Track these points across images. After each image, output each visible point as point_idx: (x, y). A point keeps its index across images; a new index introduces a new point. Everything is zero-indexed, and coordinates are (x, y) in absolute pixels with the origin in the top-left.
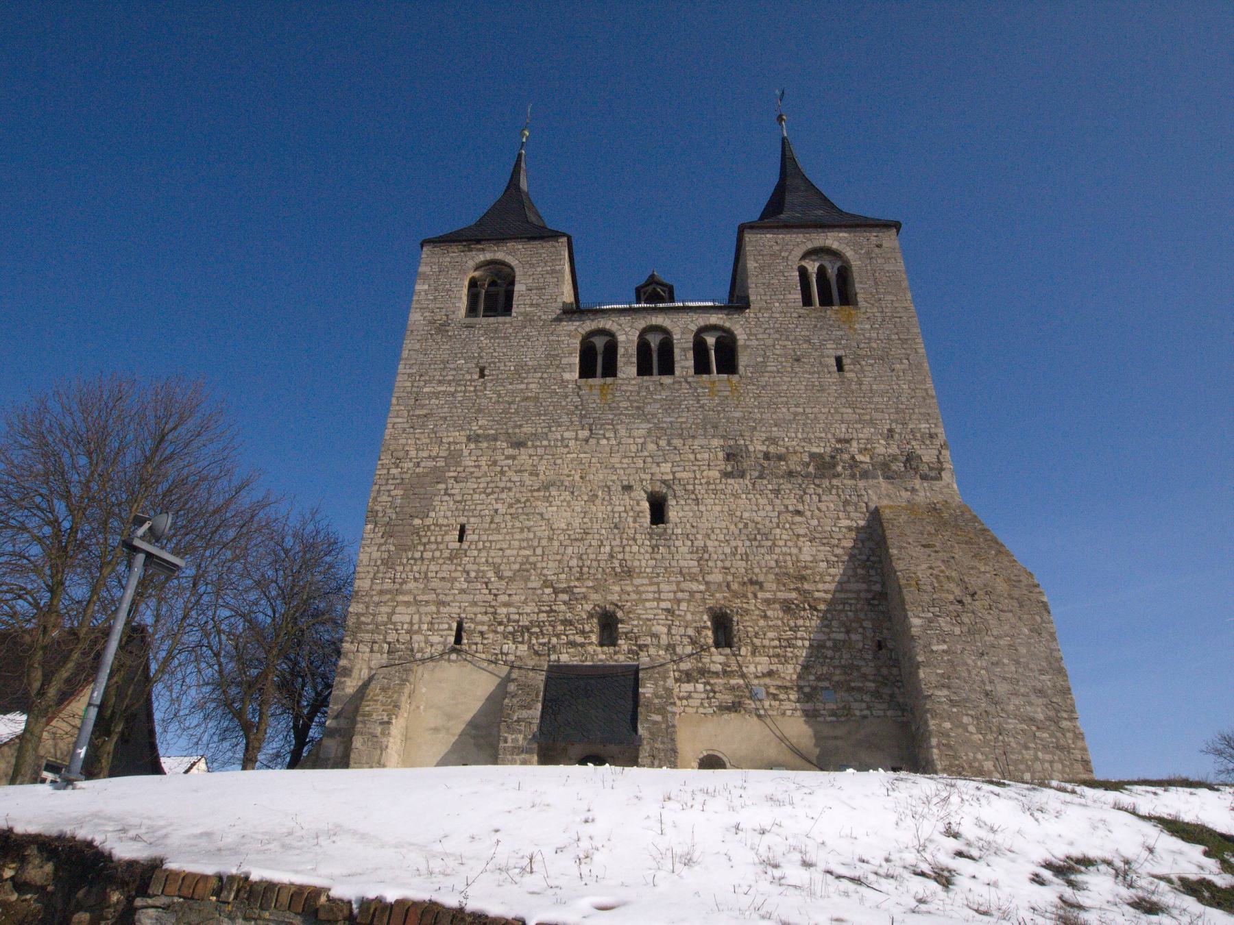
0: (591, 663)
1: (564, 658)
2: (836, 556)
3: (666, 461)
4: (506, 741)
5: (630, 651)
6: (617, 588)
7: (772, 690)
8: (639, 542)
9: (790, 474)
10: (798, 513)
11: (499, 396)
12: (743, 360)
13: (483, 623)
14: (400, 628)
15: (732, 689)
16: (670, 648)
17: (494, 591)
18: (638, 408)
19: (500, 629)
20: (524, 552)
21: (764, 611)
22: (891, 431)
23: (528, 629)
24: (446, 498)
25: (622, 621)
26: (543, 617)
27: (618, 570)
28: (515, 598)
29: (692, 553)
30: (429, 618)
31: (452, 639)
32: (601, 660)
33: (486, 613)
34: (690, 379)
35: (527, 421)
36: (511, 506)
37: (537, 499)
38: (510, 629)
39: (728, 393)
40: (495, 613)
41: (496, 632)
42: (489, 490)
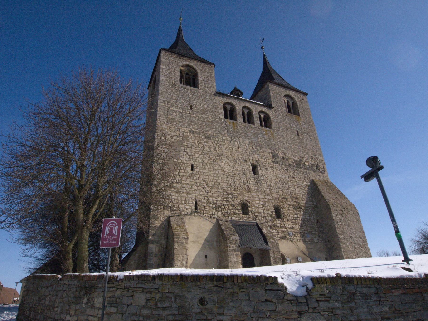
0: (242, 221)
1: (233, 218)
2: (304, 193)
3: (256, 154)
4: (230, 247)
5: (253, 217)
6: (247, 195)
7: (294, 233)
8: (252, 180)
9: (290, 165)
10: (293, 178)
11: (199, 118)
13: (204, 203)
14: (174, 201)
15: (283, 232)
16: (265, 217)
17: (207, 191)
18: (245, 134)
19: (211, 205)
20: (215, 178)
21: (288, 208)
22: (312, 157)
23: (219, 207)
24: (185, 153)
25: (250, 207)
26: (225, 202)
27: (247, 189)
28: (214, 195)
29: (267, 186)
30: (184, 199)
31: (194, 208)
32: (245, 220)
33: (205, 199)
34: (259, 128)
35: (209, 129)
36: (209, 160)
37: (217, 159)
38: (214, 206)
39: (270, 135)
40: (208, 199)
41: (209, 206)
42: (200, 153)
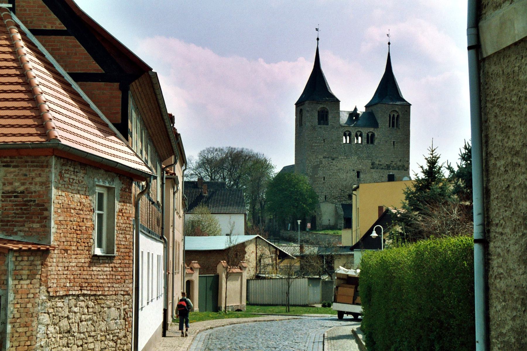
10: (383, 177)
12: (376, 142)
22: (401, 160)
23: (337, 197)
